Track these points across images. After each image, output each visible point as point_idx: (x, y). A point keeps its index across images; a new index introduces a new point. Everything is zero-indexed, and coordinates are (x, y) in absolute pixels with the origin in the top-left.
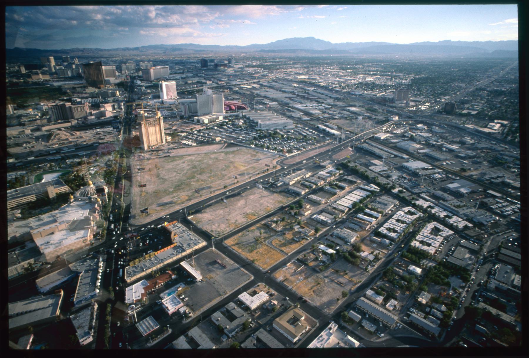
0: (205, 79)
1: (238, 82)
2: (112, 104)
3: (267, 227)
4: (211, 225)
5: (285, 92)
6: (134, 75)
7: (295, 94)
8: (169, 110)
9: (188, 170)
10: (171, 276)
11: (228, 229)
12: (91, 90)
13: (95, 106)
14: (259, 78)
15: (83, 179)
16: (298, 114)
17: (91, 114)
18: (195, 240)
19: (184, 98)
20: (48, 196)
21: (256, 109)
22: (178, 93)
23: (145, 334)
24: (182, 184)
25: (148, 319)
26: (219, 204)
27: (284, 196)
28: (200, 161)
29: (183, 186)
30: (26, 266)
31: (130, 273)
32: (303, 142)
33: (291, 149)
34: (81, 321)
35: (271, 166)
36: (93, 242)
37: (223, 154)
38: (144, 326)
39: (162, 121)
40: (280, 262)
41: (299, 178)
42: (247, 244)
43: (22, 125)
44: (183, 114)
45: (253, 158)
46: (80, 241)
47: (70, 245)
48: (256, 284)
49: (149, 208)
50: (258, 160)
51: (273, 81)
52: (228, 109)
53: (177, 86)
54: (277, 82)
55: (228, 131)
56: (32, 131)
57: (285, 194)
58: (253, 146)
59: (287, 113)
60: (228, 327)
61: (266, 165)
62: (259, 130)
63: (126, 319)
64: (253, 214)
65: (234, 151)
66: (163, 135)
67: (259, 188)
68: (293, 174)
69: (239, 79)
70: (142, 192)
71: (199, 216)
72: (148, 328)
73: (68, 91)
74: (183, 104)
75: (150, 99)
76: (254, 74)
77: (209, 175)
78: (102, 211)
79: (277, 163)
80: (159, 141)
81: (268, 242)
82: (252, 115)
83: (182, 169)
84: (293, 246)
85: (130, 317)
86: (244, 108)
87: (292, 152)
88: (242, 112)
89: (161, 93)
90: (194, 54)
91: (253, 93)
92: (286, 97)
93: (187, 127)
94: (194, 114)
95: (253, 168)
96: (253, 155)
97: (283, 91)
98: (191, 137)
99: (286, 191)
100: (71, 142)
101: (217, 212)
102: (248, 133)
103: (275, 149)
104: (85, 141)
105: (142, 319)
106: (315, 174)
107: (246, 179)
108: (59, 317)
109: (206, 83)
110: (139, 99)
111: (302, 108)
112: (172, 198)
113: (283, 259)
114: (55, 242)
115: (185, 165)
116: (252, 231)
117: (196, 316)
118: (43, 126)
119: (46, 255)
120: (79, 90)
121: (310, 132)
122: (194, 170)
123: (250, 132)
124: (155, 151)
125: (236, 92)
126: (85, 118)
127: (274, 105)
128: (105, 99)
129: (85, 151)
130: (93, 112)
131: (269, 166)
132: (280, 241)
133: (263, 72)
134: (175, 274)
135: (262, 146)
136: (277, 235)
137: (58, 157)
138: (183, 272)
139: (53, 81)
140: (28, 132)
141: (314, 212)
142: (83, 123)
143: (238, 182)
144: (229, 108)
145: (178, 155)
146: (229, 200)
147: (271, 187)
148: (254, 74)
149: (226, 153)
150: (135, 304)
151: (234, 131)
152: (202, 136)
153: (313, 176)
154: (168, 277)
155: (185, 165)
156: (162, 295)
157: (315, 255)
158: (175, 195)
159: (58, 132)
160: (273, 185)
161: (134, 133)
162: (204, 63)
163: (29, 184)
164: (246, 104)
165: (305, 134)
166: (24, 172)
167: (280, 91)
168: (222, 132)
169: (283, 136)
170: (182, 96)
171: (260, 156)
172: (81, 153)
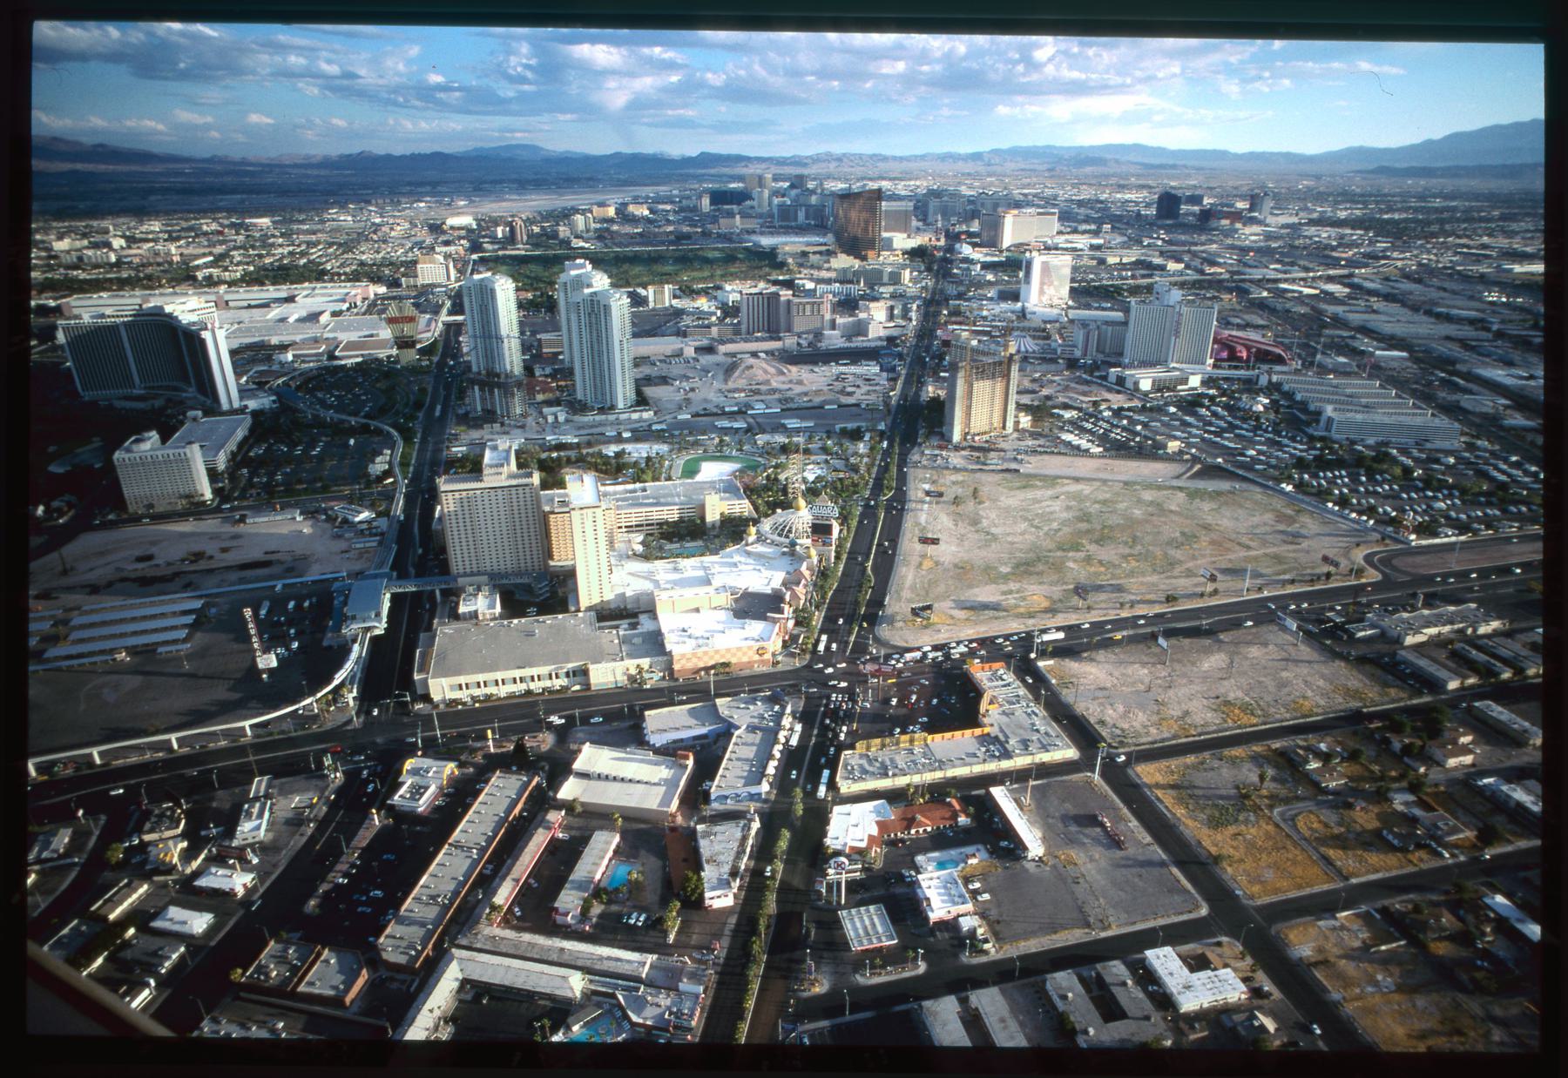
0: (1162, 254)
1: (1272, 270)
2: (890, 303)
3: (1288, 764)
4: (1101, 704)
5: (1448, 318)
6: (958, 229)
7: (1488, 330)
8: (1039, 338)
9: (1064, 523)
10: (955, 816)
11: (1153, 731)
12: (843, 261)
13: (848, 305)
14: (1351, 263)
15: (785, 491)
16: (1487, 403)
17: (833, 326)
18: (1046, 734)
19: (1088, 307)
20: (703, 518)
21: (1320, 366)
22: (1072, 290)
23: (856, 947)
24: (1039, 559)
25: (872, 908)
26: (1141, 646)
27: (1372, 677)
28: (1104, 502)
29: (1040, 567)
30: (633, 671)
31: (852, 772)
32: (1489, 504)
33: (1434, 520)
34: (717, 847)
35: (1344, 563)
36: (780, 658)
37: (1181, 495)
38: (858, 925)
39: (1015, 368)
40: (1311, 896)
41: (1447, 628)
42: (1208, 798)
43: (682, 334)
44: (1078, 353)
45: (1281, 527)
46: (750, 648)
47: (728, 650)
48: (1215, 936)
49: (936, 605)
50: (1296, 537)
51: (1407, 276)
52: (1225, 355)
53: (1075, 269)
54: (1419, 281)
55: (1211, 424)
56: (697, 350)
57: (1379, 672)
58: (1290, 488)
59: (1442, 394)
60: (1091, 1031)
61: (1325, 559)
62: (1322, 439)
63: (818, 887)
64: (1245, 708)
65: (1219, 494)
66: (1012, 407)
67: (1285, 629)
68: (1426, 612)
69: (1278, 261)
70: (924, 556)
71: (1072, 666)
72: (867, 934)
73: (790, 260)
74: (1084, 324)
75: (991, 299)
76: (1334, 249)
77: (1127, 551)
78: (815, 585)
79: (1368, 559)
80: (997, 422)
81: (1282, 814)
82: (1304, 385)
83: (1047, 517)
84: (1374, 858)
85: (830, 887)
86: (1279, 360)
87: (1436, 535)
88: (1270, 373)
89: (1023, 287)
90: (1138, 176)
91: (1321, 313)
92: (1448, 338)
93: (1085, 394)
94: (1112, 360)
95: (1278, 559)
96: (1281, 517)
97: (1438, 316)
98: (1089, 426)
99: (1383, 660)
100: (774, 391)
101: (1129, 671)
102: (1278, 443)
103: (1371, 511)
104: (806, 394)
105: (859, 904)
106: (1522, 631)
107: (1244, 590)
108: (673, 816)
109: (1162, 268)
110: (960, 296)
111: (1509, 381)
112: (1004, 593)
113: (1326, 887)
114: (698, 634)
115: (1056, 506)
116: (1233, 761)
117: (1000, 956)
118: (723, 342)
119: (676, 658)
120: (814, 259)
121: (1526, 473)
122: (1084, 526)
123: (1286, 441)
124: (981, 450)
125: (1261, 305)
126: (818, 335)
127: (1393, 359)
128: (872, 289)
129: (802, 418)
130: (840, 320)
131: (1336, 565)
132: (1326, 825)
133: (1372, 242)
134: (967, 815)
135: (1322, 495)
136: (1319, 803)
137: (739, 424)
138: (992, 817)
139: (762, 233)
140: (689, 352)
141: (1487, 765)
142: (810, 345)
143: (1216, 592)
144: (1228, 352)
145: (1047, 472)
146: (1173, 641)
147: (1328, 636)
148: (1334, 249)
149: (1193, 495)
150: (848, 856)
151: (1232, 427)
152: (1124, 429)
153: (1508, 634)
154: (948, 815)
155: (1056, 506)
156: (920, 859)
157: (1460, 919)
158: (1013, 586)
159: (752, 361)
160: (1335, 632)
161: (930, 389)
162: (1169, 203)
163: (669, 478)
164: (1288, 348)
165: (1503, 478)
166: (665, 448)
167: (1428, 313)
168: (1190, 425)
169: (1407, 471)
170: (1083, 300)
171: (1309, 524)
172: (792, 423)
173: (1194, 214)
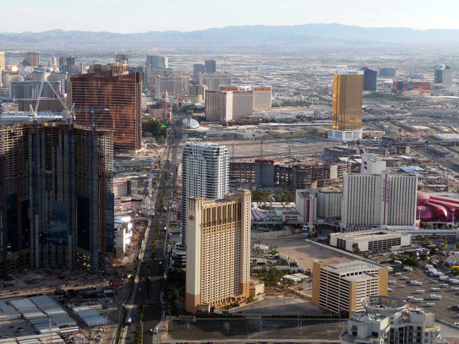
94: (332, 224)
173: (389, 85)
